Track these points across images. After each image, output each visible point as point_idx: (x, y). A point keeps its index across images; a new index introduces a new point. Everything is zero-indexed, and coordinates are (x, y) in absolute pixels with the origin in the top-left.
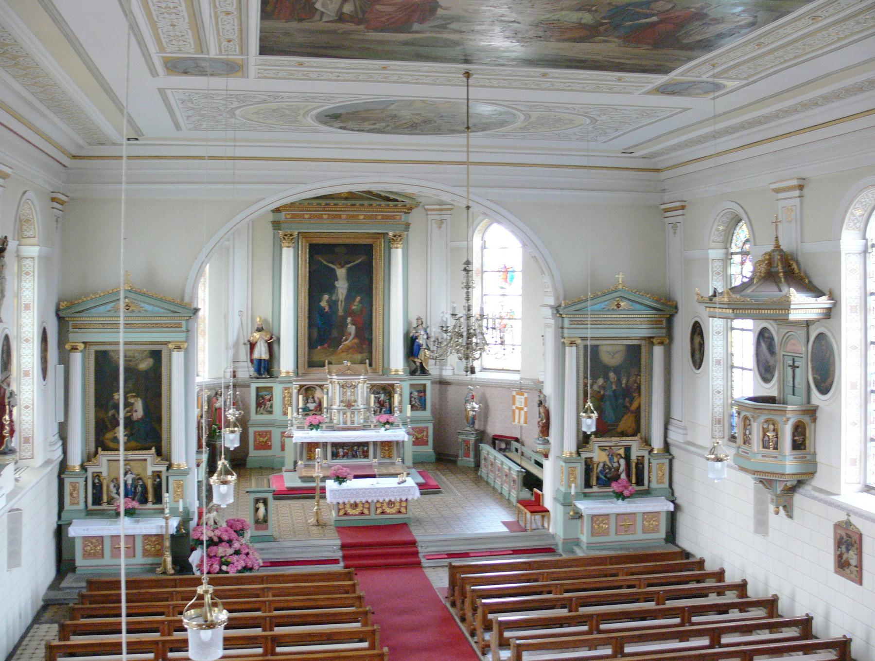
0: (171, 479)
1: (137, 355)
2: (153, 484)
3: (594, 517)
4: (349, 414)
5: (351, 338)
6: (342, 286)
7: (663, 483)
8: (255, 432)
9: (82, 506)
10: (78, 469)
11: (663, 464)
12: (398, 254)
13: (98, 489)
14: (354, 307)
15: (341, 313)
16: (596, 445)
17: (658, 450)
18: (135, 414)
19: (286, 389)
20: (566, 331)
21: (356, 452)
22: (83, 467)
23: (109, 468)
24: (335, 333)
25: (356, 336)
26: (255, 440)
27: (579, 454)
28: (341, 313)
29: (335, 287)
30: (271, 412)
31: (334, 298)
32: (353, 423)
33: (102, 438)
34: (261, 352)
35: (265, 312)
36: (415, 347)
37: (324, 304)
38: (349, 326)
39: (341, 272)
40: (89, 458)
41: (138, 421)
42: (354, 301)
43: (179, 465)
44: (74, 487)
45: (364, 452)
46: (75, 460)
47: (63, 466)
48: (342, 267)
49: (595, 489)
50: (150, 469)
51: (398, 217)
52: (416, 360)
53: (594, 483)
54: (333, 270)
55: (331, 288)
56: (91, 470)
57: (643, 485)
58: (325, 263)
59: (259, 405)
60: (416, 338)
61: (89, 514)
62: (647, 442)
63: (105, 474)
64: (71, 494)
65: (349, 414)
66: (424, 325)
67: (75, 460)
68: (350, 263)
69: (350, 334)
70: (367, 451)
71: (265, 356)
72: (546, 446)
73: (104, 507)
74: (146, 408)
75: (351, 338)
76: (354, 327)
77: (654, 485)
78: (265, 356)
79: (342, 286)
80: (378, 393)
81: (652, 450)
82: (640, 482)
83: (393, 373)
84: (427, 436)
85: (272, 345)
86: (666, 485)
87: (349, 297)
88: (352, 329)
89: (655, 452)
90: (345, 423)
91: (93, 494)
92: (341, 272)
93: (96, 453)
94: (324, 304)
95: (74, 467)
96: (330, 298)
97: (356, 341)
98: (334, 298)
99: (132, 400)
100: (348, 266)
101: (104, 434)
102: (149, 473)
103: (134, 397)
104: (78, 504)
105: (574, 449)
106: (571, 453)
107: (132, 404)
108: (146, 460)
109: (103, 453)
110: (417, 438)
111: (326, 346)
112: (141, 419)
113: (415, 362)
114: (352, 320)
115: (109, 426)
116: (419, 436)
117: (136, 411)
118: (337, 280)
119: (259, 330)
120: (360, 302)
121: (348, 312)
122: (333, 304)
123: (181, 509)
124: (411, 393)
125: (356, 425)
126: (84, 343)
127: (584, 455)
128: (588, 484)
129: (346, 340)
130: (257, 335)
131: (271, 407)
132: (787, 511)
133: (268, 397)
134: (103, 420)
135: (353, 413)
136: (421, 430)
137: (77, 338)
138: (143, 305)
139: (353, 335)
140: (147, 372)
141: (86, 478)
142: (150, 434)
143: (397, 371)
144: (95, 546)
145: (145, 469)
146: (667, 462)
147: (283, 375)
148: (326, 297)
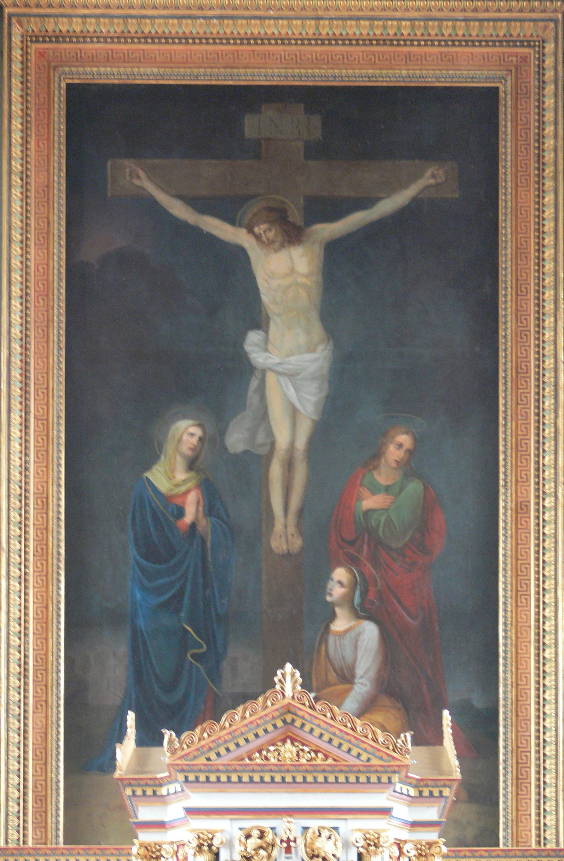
6: (290, 363)
14: (370, 502)
15: (284, 535)
28: (284, 535)
29: (241, 369)
31: (236, 440)
37: (169, 476)
38: (341, 624)
39: (285, 273)
48: (293, 235)
54: (235, 263)
55: (218, 379)
58: (179, 210)
68: (332, 210)
76: (370, 631)
79: (290, 363)
87: (341, 435)
92: (285, 273)
94: (169, 476)
96: (213, 441)
98: (236, 440)
100: (328, 230)
114: (361, 583)
118: (257, 319)
120: (411, 467)
121: (334, 531)
122: (231, 478)
139: (362, 687)
148: (186, 433)
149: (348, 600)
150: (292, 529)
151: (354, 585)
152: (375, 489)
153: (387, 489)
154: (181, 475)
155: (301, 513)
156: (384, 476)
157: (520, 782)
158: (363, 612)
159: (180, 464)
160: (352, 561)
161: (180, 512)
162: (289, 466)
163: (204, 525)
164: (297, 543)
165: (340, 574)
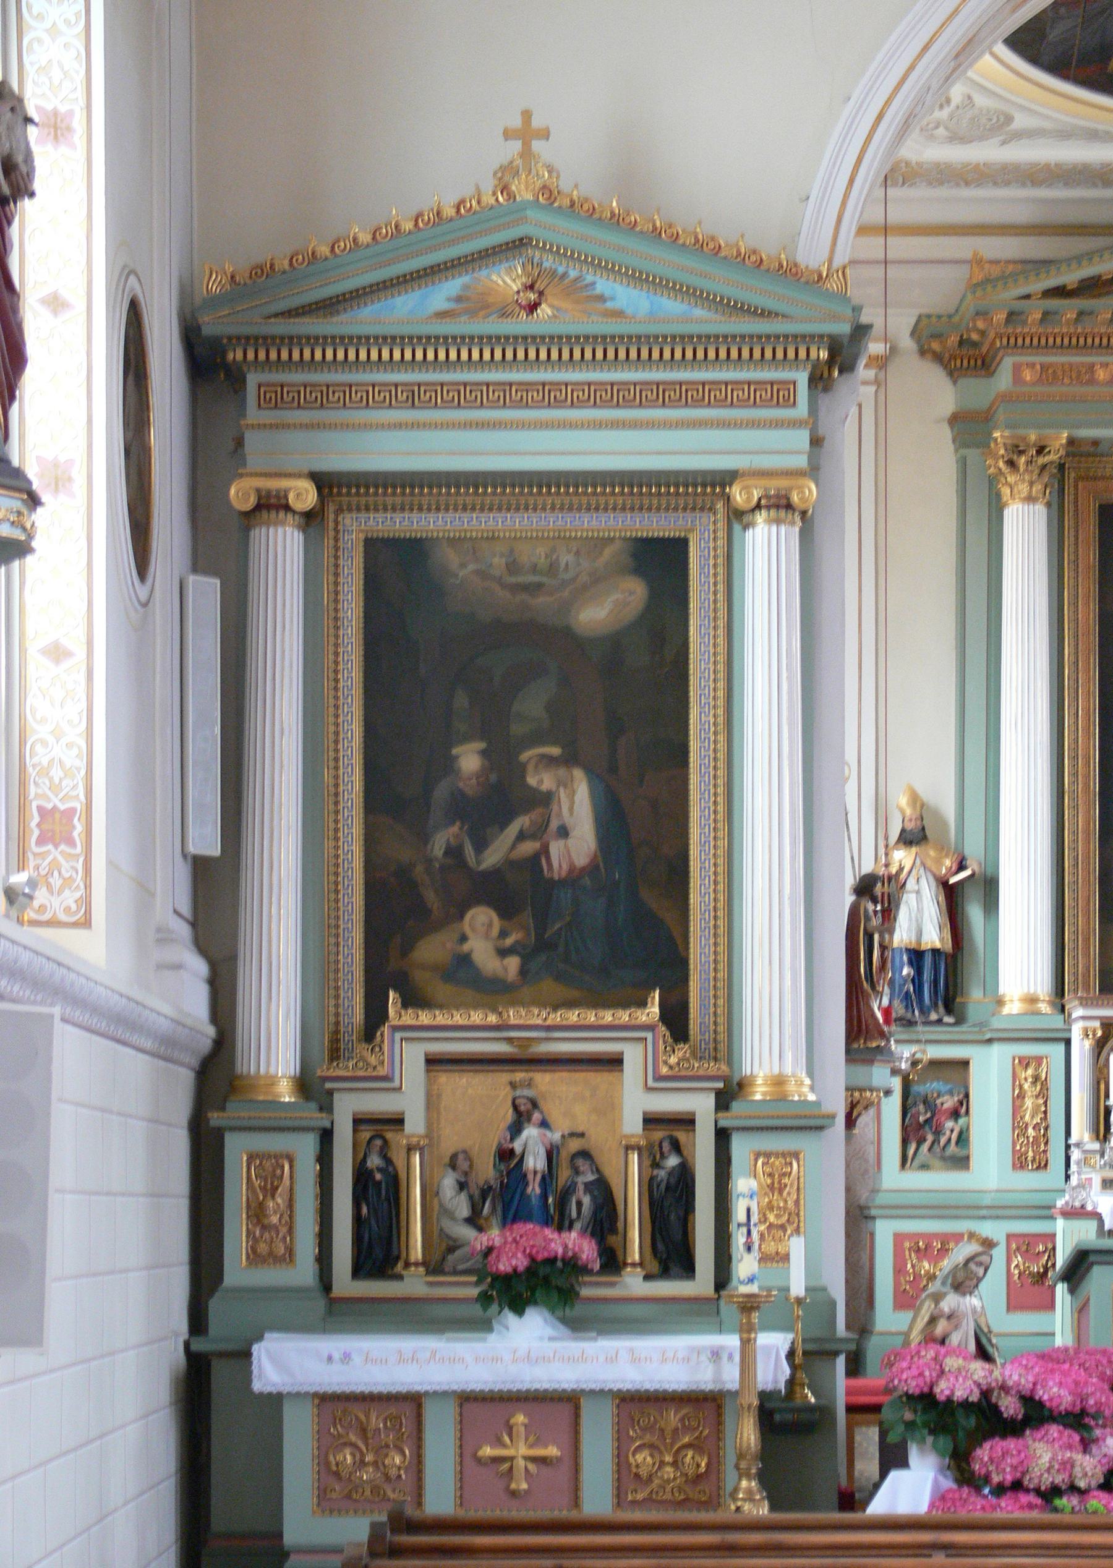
0: (741, 1148)
1: (566, 558)
2: (650, 1186)
8: (899, 1239)
9: (303, 1271)
10: (285, 1093)
13: (380, 1195)
18: (556, 848)
19: (1025, 1062)
22: (306, 1085)
23: (432, 1102)
26: (899, 1270)
30: (962, 1162)
33: (393, 943)
34: (919, 921)
35: (928, 772)
40: (336, 1049)
41: (574, 879)
43: (779, 1081)
44: (269, 1174)
46: (276, 1050)
47: (216, 1076)
50: (635, 1099)
56: (347, 1106)
59: (911, 1132)
61: (335, 1313)
63: (415, 1125)
64: (257, 1213)
67: (276, 1050)
71: (934, 936)
73: (414, 1284)
74: (612, 818)
78: (934, 936)
85: (967, 895)
91: (358, 1221)
93: (375, 1016)
95: (272, 1080)
99: (542, 780)
101: (406, 949)
102: (632, 1125)
103: (550, 761)
104: (289, 1256)
107: (545, 799)
108: (615, 1062)
109: (409, 1017)
112: (592, 869)
115: (431, 898)
117: (564, 832)
119: (911, 838)
123: (798, 1288)
126: (323, 482)
130: (902, 857)
131: (963, 1139)
133: (949, 1102)
134: (404, 873)
137: (289, 453)
138: (603, 285)
140: (614, 644)
141: (326, 1136)
142: (636, 932)
144: (382, 1450)
145: (610, 1108)
147: (1013, 1008)
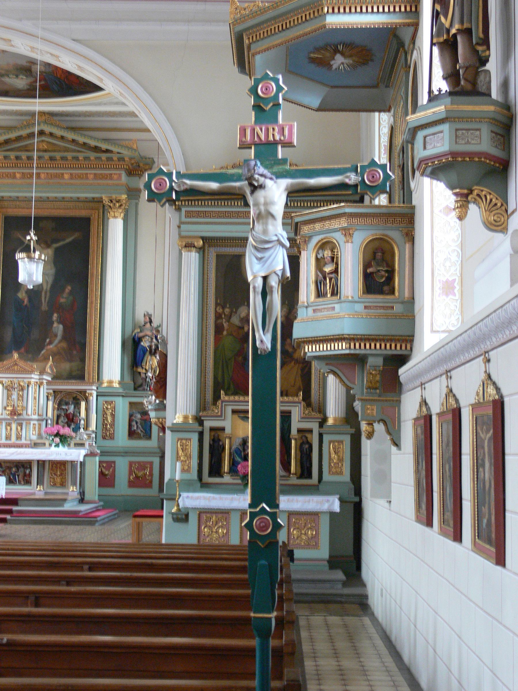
3: (204, 514)
4: (14, 426)
5: (56, 342)
7: (341, 473)
11: (342, 442)
12: (116, 227)
14: (62, 300)
15: (44, 307)
16: (229, 409)
17: (335, 419)
20: (183, 227)
21: (14, 475)
24: (35, 334)
25: (64, 338)
27: (199, 421)
28: (44, 307)
32: (19, 437)
36: (139, 352)
38: (55, 325)
42: (63, 291)
45: (25, 475)
49: (227, 479)
51: (115, 177)
52: (140, 370)
53: (226, 468)
57: (309, 476)
60: (140, 339)
62: (322, 409)
65: (14, 426)
66: (155, 324)
69: (56, 336)
70: (30, 475)
72: (161, 414)
75: (56, 342)
76: (61, 327)
77: (326, 477)
80: (67, 404)
81: (325, 419)
82: (305, 472)
83: (105, 385)
84: (151, 474)
86: (346, 476)
88: (58, 328)
89: (330, 422)
90: (8, 438)
97: (64, 345)
105: (192, 412)
106: (186, 417)
110: (137, 477)
111: (23, 350)
113: (140, 373)
114: (60, 317)
116: (140, 474)
120: (71, 293)
121: (54, 306)
124: (131, 416)
125: (23, 441)
127: (208, 424)
128: (216, 470)
129: (50, 343)
132: (388, 432)
135: (21, 425)
136: (142, 466)
139: (59, 337)
143: (110, 382)
146: (347, 440)
149: (57, 320)
150: (46, 305)
151: (58, 317)
152: (63, 298)
153: (66, 298)
154: (24, 295)
155: (48, 303)
156: (65, 295)
157: (90, 358)
158: (59, 322)
159: (24, 292)
160: (58, 312)
161: (24, 302)
162: (46, 293)
163: (28, 305)
164: (47, 309)
165: (55, 315)
